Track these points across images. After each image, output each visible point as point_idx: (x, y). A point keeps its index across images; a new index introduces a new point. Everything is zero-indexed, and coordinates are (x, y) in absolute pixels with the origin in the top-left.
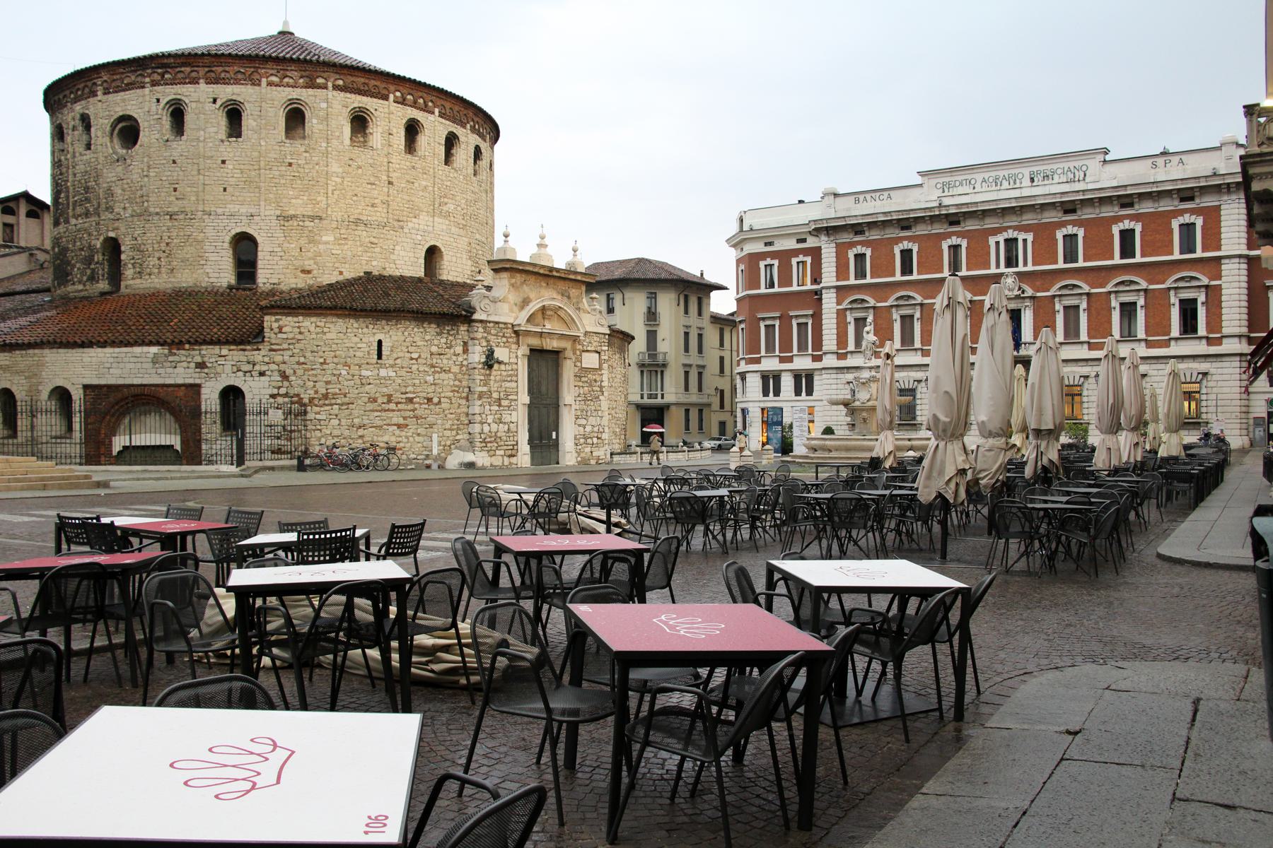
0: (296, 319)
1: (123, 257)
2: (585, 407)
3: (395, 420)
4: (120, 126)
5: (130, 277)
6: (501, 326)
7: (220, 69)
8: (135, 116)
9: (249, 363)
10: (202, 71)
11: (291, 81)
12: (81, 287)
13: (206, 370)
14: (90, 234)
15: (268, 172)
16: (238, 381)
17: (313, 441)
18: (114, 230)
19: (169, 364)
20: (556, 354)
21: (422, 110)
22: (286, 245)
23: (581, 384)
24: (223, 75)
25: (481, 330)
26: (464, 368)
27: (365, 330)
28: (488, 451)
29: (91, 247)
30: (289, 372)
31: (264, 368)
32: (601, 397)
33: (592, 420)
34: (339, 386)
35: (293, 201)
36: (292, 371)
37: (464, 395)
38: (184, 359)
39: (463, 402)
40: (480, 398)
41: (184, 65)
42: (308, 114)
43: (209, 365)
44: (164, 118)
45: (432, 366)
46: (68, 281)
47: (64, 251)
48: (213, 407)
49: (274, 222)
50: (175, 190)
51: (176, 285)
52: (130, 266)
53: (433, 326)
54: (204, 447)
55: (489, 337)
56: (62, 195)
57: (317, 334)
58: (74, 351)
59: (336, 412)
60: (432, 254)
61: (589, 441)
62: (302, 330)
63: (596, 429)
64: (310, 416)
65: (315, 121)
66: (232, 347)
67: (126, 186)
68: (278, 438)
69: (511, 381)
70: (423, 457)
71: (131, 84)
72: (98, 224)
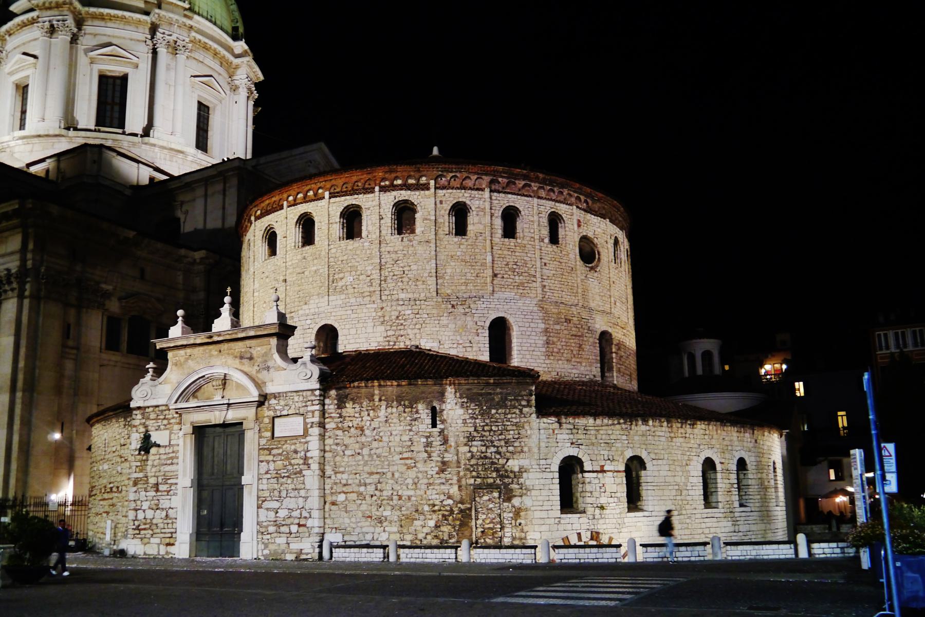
2: (276, 486)
6: (161, 408)
20: (234, 430)
23: (270, 458)
25: (139, 417)
28: (142, 539)
33: (290, 503)
45: (121, 457)
55: (147, 423)
61: (284, 529)
69: (172, 464)
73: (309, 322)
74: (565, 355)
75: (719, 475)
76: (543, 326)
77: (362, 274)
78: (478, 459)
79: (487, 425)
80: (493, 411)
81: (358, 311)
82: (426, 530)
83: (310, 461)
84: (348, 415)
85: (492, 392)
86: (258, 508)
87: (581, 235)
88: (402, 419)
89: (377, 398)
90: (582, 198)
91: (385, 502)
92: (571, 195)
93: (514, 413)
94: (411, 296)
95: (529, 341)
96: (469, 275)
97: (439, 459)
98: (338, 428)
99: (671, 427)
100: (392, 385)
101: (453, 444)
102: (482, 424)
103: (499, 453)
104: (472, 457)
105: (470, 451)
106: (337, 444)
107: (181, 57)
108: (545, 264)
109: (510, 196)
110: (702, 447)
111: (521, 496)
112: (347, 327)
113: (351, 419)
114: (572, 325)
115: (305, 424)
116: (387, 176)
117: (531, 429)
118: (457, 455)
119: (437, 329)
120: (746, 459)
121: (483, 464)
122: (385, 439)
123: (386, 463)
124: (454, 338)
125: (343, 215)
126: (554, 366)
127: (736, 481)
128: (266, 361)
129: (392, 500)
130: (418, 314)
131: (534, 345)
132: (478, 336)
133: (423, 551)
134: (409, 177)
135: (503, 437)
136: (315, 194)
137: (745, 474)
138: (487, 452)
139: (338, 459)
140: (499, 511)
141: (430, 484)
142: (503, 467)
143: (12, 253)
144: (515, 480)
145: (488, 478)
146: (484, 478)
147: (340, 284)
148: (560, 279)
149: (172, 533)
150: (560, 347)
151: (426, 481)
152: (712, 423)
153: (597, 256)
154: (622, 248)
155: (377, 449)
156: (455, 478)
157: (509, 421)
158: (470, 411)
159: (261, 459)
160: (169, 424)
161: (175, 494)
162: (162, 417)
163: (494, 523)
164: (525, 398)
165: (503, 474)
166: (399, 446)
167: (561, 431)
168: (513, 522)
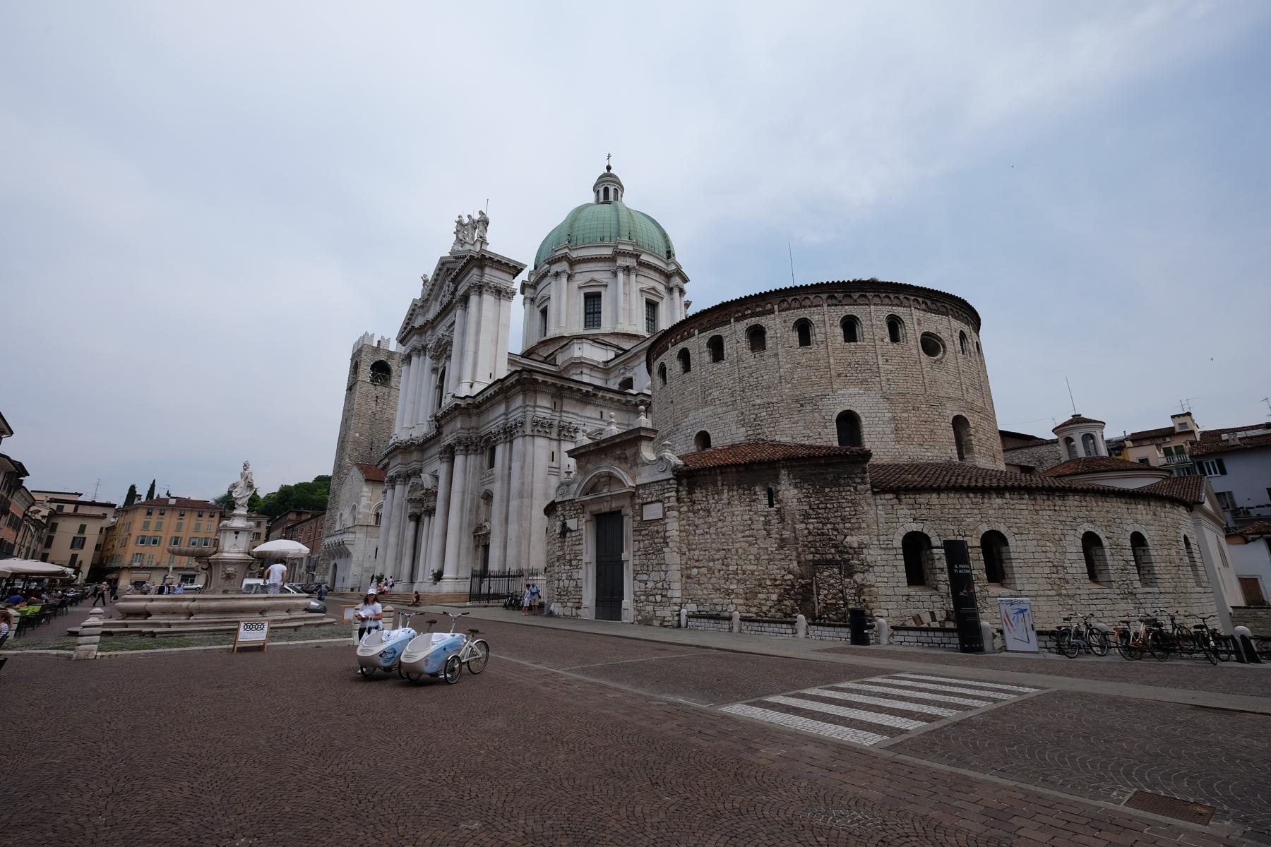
23: (640, 538)
25: (560, 509)
63: (659, 585)
69: (579, 544)
73: (689, 431)
74: (916, 440)
75: (1107, 552)
76: (890, 415)
77: (725, 388)
78: (815, 536)
79: (822, 503)
80: (827, 490)
81: (724, 418)
82: (769, 603)
83: (668, 540)
84: (697, 499)
85: (824, 471)
86: (634, 580)
87: (923, 331)
88: (742, 500)
89: (719, 483)
90: (920, 300)
91: (731, 576)
92: (908, 299)
93: (848, 491)
94: (766, 400)
95: (877, 429)
96: (814, 378)
97: (777, 536)
98: (689, 511)
99: (1035, 499)
100: (731, 472)
101: (790, 522)
102: (816, 502)
103: (837, 530)
104: (810, 533)
105: (807, 529)
106: (689, 525)
107: (633, 277)
108: (887, 361)
109: (847, 307)
110: (1078, 520)
111: (863, 573)
112: (717, 431)
113: (699, 502)
114: (921, 412)
115: (664, 508)
116: (739, 308)
117: (869, 505)
118: (794, 532)
119: (789, 426)
120: (1143, 532)
121: (820, 540)
122: (729, 519)
123: (731, 540)
124: (805, 431)
125: (709, 345)
126: (905, 450)
127: (1133, 558)
128: (635, 459)
129: (737, 574)
130: (772, 414)
131: (882, 433)
132: (826, 428)
133: (761, 624)
134: (758, 306)
135: (840, 514)
136: (688, 334)
137: (1144, 550)
138: (823, 529)
139: (691, 537)
140: (841, 587)
141: (771, 559)
142: (842, 543)
143: (518, 408)
144: (855, 556)
145: (826, 554)
146: (823, 554)
147: (710, 398)
148: (904, 372)
149: (579, 599)
150: (910, 433)
151: (767, 557)
152: (1089, 495)
153: (942, 349)
154: (970, 341)
155: (723, 528)
156: (794, 554)
157: (844, 498)
158: (804, 491)
159: (635, 539)
160: (577, 513)
161: (581, 568)
162: (573, 508)
163: (835, 599)
164: (859, 475)
165: (842, 549)
166: (741, 525)
167: (900, 507)
168: (856, 598)
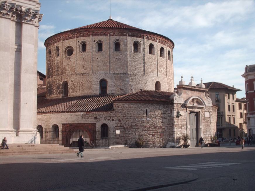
0: (122, 104)
1: (69, 87)
3: (151, 133)
4: (68, 49)
5: (71, 92)
7: (97, 32)
8: (72, 46)
9: (109, 117)
10: (91, 33)
11: (116, 34)
12: (56, 95)
13: (97, 119)
14: (59, 80)
15: (110, 61)
16: (106, 122)
17: (128, 140)
18: (66, 79)
19: (86, 118)
21: (153, 41)
22: (116, 82)
23: (204, 122)
24: (97, 33)
25: (176, 106)
26: (171, 118)
27: (142, 107)
29: (59, 84)
30: (121, 119)
31: (114, 118)
32: (211, 126)
34: (135, 123)
35: (118, 69)
36: (122, 119)
37: (171, 125)
38: (90, 116)
39: (171, 128)
40: (176, 126)
41: (86, 31)
42: (121, 44)
43: (98, 118)
44: (80, 46)
46: (52, 94)
47: (51, 85)
48: (99, 130)
49: (112, 76)
50: (84, 67)
51: (85, 95)
52: (71, 89)
53: (162, 105)
54: (96, 142)
56: (51, 69)
57: (129, 108)
58: (59, 114)
59: (135, 131)
60: (158, 84)
62: (124, 107)
64: (127, 132)
65: (123, 46)
66: (105, 112)
67: (70, 66)
68: (118, 139)
70: (160, 144)
71: (71, 37)
72: (61, 77)
73: (154, 79)
83: (211, 123)
